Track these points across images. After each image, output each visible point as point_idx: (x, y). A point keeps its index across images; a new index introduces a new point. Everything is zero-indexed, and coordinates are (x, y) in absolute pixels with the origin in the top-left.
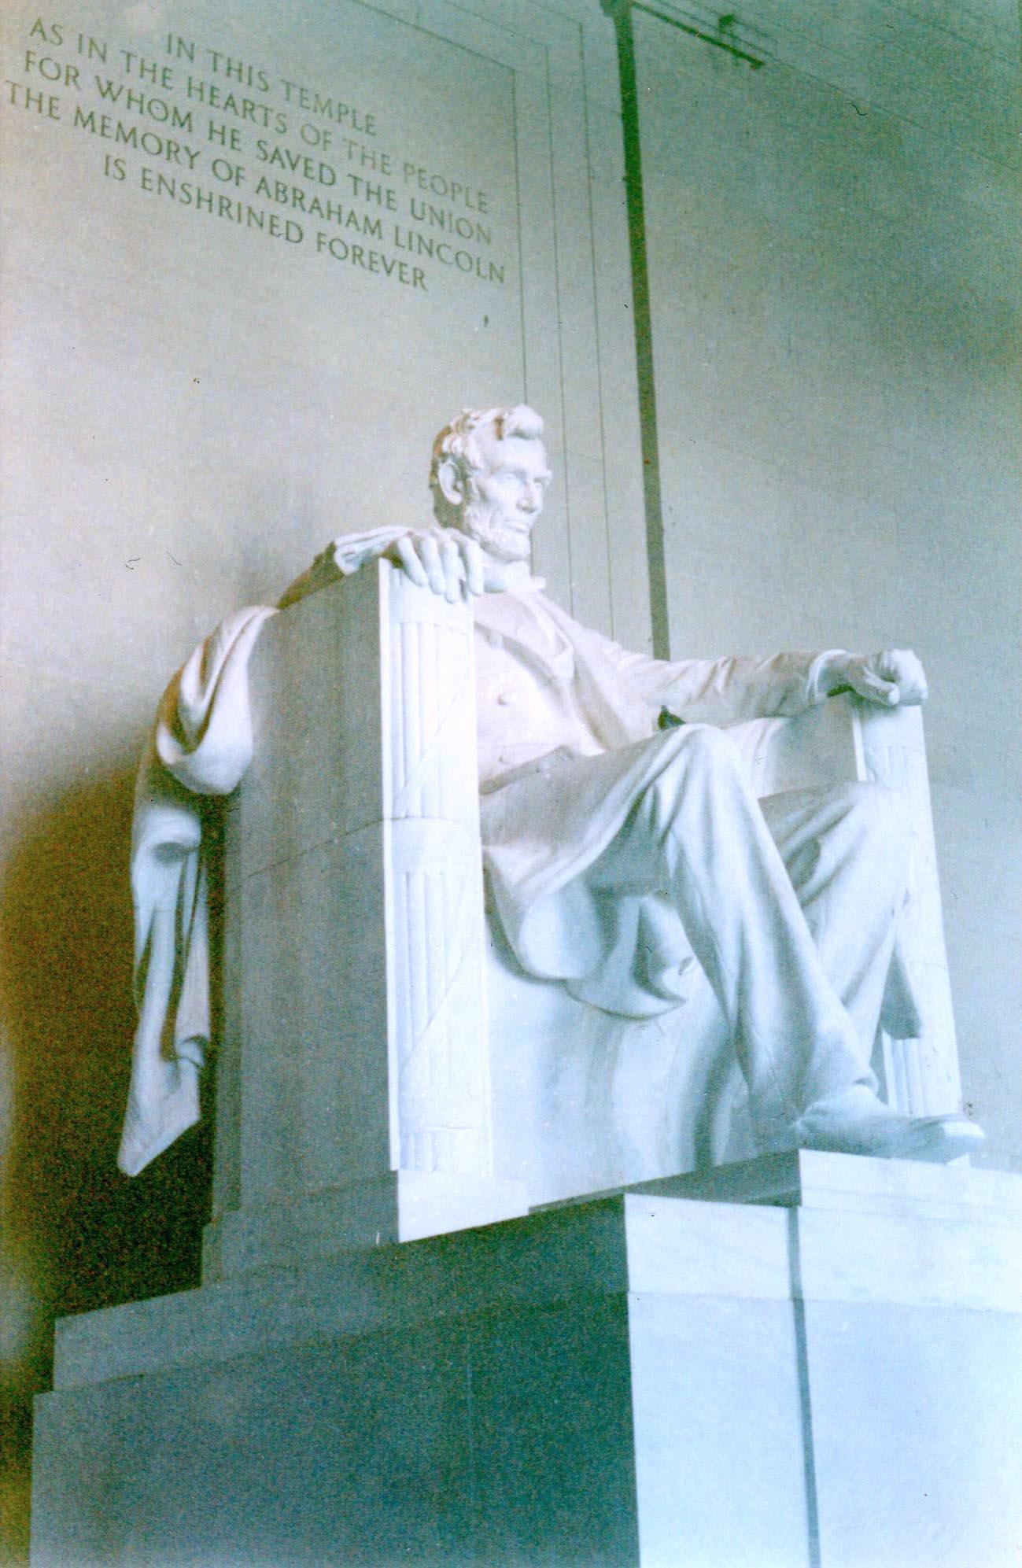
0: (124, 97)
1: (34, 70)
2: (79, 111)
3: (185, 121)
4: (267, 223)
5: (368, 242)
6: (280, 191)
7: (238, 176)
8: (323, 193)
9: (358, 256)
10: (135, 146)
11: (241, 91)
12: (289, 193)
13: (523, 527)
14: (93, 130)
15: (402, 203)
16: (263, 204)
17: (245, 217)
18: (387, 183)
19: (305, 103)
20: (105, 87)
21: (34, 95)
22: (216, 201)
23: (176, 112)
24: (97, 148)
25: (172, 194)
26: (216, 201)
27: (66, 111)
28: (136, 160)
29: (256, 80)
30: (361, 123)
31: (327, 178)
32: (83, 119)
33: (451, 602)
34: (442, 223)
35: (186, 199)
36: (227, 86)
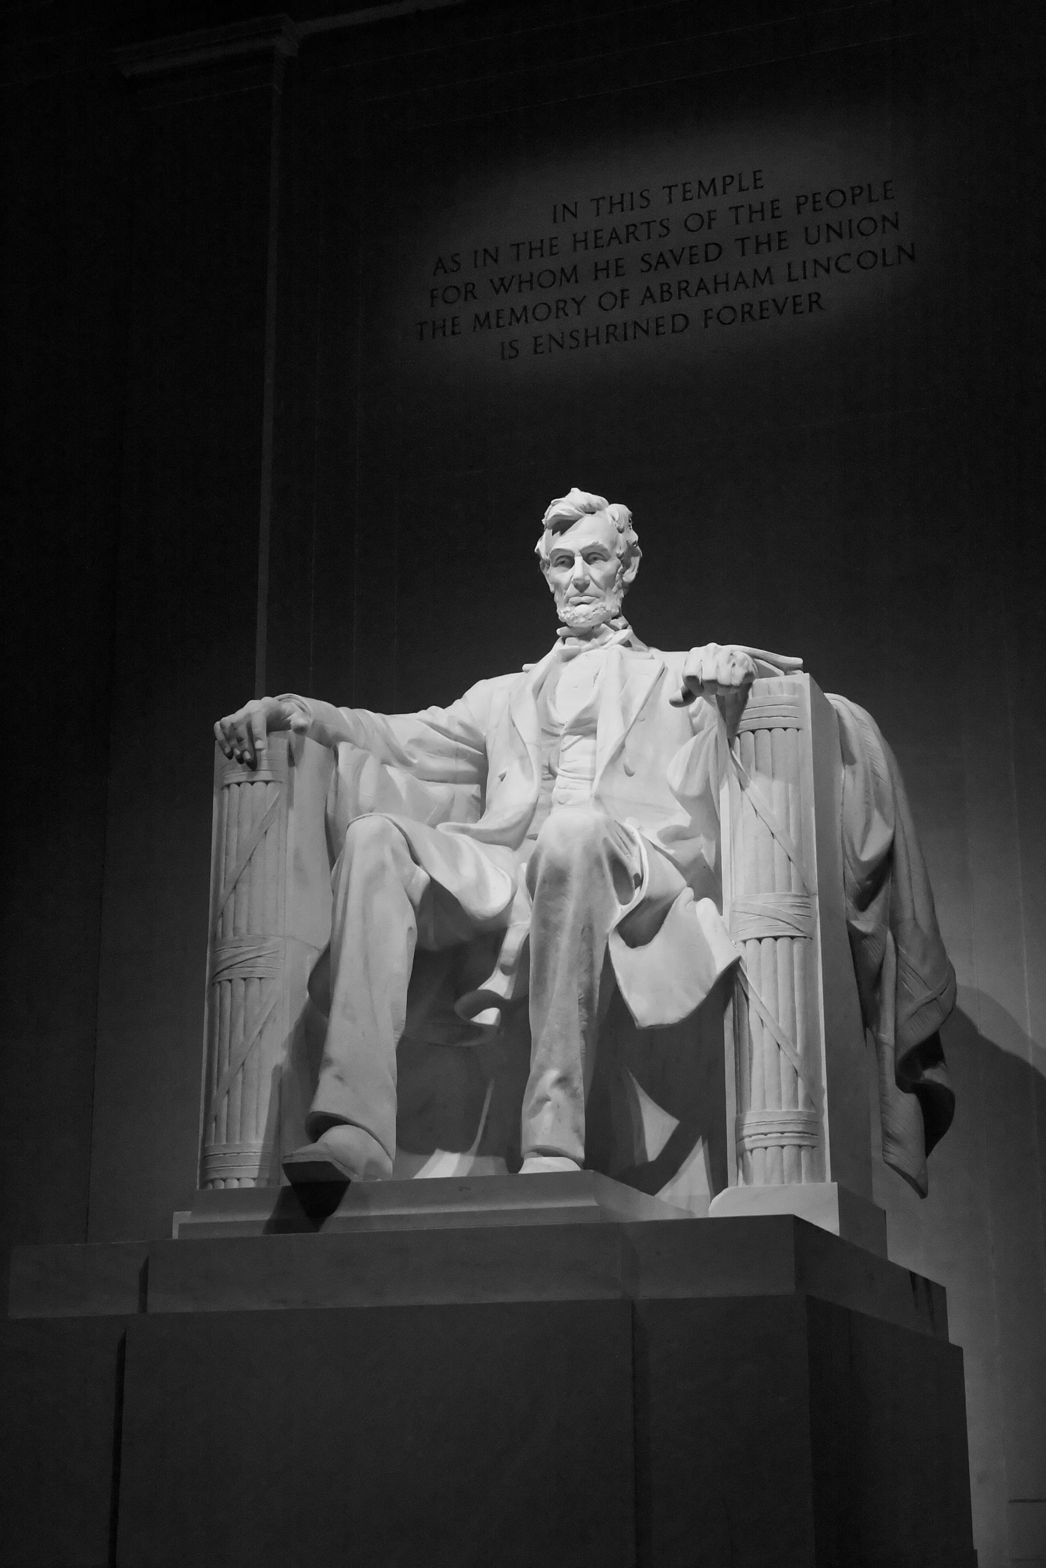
0: (515, 287)
2: (477, 317)
3: (570, 275)
7: (623, 299)
10: (526, 321)
12: (674, 290)
13: (584, 599)
14: (490, 327)
17: (630, 333)
19: (688, 195)
23: (563, 270)
25: (562, 346)
30: (748, 182)
31: (713, 252)
32: (482, 322)
34: (840, 236)
35: (574, 343)
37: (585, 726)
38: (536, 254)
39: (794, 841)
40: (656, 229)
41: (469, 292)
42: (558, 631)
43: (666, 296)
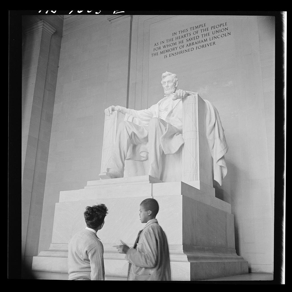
1: (155, 50)
4: (188, 51)
5: (204, 43)
6: (190, 44)
8: (196, 41)
9: (203, 46)
11: (183, 34)
12: (191, 44)
15: (211, 34)
16: (188, 48)
17: (184, 52)
18: (207, 32)
20: (164, 46)
21: (155, 54)
22: (180, 52)
24: (163, 55)
26: (180, 52)
27: (159, 53)
28: (168, 54)
29: (186, 31)
30: (203, 25)
31: (198, 37)
33: (109, 116)
36: (181, 35)
37: (166, 109)
38: (170, 41)
39: (194, 122)
40: (189, 35)
41: (160, 48)
42: (165, 95)
43: (190, 45)
